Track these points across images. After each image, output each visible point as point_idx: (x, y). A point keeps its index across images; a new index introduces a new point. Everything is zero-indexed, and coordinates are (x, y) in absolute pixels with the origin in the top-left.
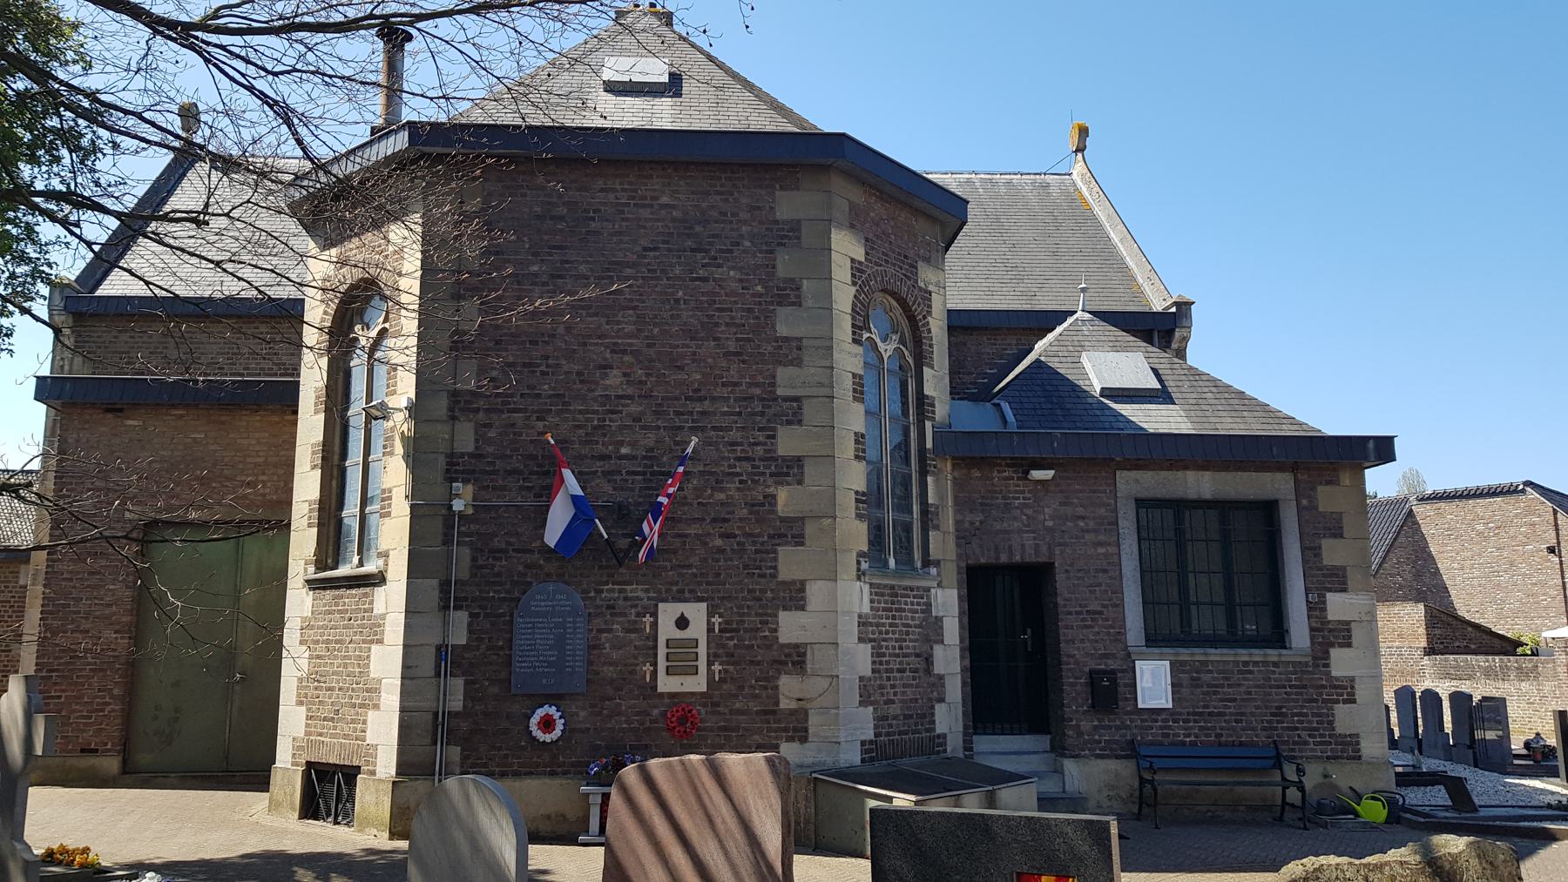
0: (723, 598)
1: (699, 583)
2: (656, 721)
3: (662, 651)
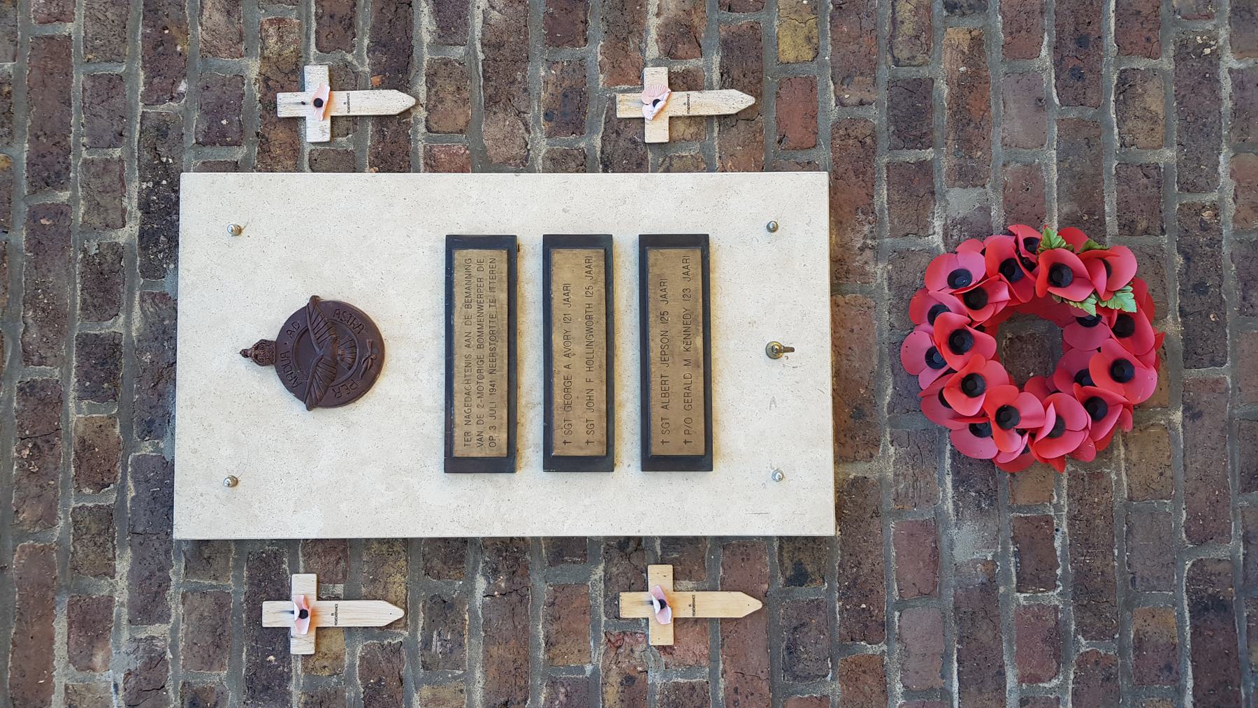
0: (163, 60)
1: (49, 235)
3: (534, 505)
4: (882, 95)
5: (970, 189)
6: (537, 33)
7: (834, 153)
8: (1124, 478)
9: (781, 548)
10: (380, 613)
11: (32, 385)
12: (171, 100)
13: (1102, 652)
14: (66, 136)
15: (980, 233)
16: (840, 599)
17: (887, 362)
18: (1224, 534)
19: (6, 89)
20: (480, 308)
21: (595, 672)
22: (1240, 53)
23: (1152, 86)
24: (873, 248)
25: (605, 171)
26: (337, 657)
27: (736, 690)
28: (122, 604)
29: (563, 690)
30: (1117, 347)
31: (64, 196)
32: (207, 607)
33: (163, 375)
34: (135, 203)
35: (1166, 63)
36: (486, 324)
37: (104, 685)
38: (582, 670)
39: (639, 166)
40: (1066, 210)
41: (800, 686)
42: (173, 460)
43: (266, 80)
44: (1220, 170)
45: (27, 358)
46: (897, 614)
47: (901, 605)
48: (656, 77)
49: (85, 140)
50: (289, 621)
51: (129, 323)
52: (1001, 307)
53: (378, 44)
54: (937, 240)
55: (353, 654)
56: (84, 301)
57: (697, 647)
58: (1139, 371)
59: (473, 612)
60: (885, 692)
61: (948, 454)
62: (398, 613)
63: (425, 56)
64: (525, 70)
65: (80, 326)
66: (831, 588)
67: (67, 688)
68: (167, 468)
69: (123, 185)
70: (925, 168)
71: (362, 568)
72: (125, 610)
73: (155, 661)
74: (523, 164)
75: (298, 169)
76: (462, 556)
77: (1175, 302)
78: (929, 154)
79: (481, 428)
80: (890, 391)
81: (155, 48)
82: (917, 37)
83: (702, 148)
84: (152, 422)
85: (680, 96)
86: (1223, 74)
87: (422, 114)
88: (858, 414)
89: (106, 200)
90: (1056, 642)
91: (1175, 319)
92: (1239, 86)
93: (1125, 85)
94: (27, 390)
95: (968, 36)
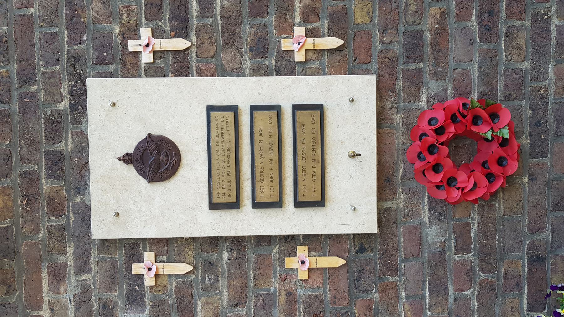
1: (29, 106)
2: (462, 232)
3: (248, 222)
4: (401, 38)
5: (439, 81)
6: (245, 11)
7: (379, 65)
8: (502, 206)
9: (354, 238)
10: (183, 268)
11: (26, 173)
12: (80, 44)
13: (490, 279)
14: (33, 61)
15: (442, 99)
16: (379, 259)
17: (401, 158)
18: (543, 229)
19: (5, 40)
20: (223, 138)
21: (275, 290)
22: (560, 17)
23: (521, 34)
24: (395, 107)
25: (277, 75)
26: (165, 287)
27: (335, 297)
28: (71, 266)
29: (261, 298)
30: (501, 152)
31: (34, 88)
32: (108, 266)
33: (84, 166)
34: (66, 91)
35: (527, 23)
36: (225, 145)
37: (65, 300)
38: (270, 290)
39: (292, 72)
40: (481, 90)
41: (362, 295)
42: (90, 204)
43: (123, 34)
44: (549, 71)
45: (23, 161)
46: (403, 264)
47: (405, 261)
48: (299, 31)
49: (42, 63)
50: (144, 272)
51: (67, 145)
52: (451, 135)
53: (173, 17)
54: (423, 104)
55: (171, 285)
56: (46, 136)
57: (318, 279)
58: (510, 161)
59: (223, 267)
60: (398, 297)
61: (426, 197)
62: (190, 268)
63: (195, 23)
64: (240, 28)
65: (45, 146)
66: (375, 255)
67: (49, 301)
68: (88, 208)
69: (61, 83)
70: (420, 72)
71: (174, 249)
72: (72, 268)
73: (86, 290)
74: (239, 72)
75: (139, 76)
76: (217, 243)
77: (527, 130)
78: (421, 65)
79: (224, 190)
80: (402, 170)
81: (71, 20)
82: (417, 12)
83: (320, 64)
84: (79, 188)
85: (310, 40)
86: (553, 27)
87: (194, 49)
88: (388, 180)
89: (53, 90)
90: (470, 276)
91: (526, 137)
92: (560, 33)
93: (509, 34)
94: (23, 175)
95: (440, 11)
